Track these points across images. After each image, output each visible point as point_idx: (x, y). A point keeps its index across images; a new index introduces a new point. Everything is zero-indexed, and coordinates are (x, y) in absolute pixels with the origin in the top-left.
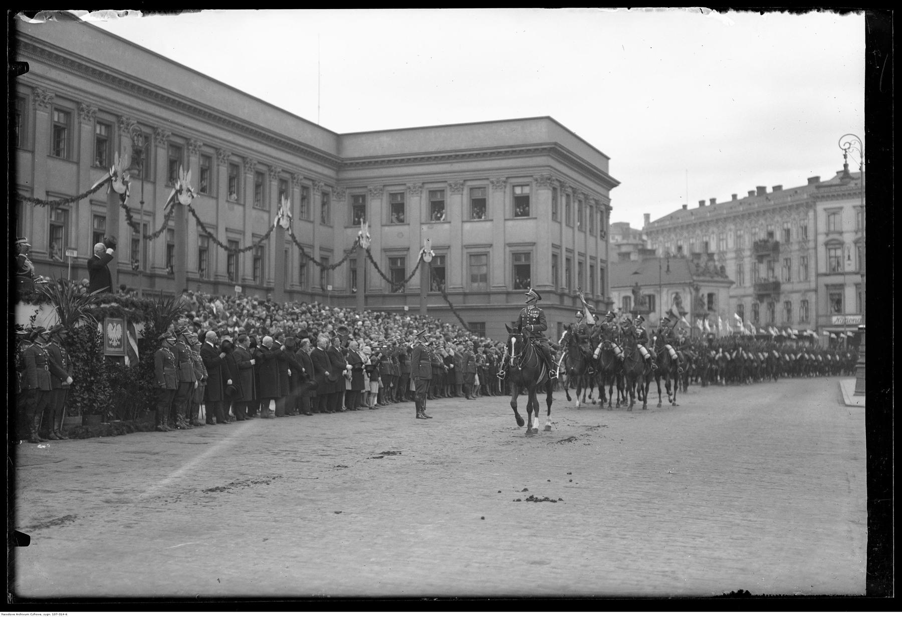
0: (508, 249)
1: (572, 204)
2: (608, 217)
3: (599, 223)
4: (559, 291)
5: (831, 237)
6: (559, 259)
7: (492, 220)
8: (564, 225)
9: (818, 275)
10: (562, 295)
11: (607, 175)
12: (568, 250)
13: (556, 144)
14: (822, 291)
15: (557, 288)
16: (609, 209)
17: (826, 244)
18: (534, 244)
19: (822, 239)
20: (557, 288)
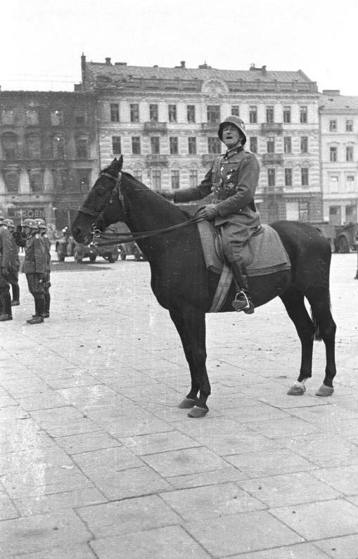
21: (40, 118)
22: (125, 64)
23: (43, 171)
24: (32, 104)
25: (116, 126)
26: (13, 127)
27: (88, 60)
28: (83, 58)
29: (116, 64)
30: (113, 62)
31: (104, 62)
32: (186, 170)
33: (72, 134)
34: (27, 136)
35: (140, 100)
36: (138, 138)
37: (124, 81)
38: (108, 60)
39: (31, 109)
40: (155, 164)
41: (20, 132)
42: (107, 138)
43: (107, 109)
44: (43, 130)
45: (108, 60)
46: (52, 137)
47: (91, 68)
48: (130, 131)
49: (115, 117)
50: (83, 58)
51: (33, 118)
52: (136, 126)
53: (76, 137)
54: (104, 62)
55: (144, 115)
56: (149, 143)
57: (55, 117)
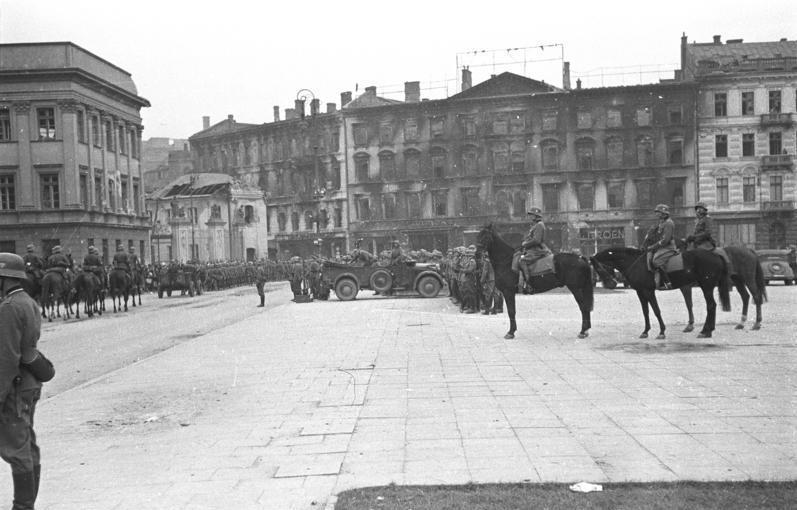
0: (34, 171)
1: (99, 125)
2: (140, 136)
3: (130, 145)
4: (89, 210)
5: (360, 150)
6: (88, 180)
7: (17, 142)
8: (91, 146)
9: (348, 186)
10: (93, 213)
11: (136, 96)
12: (97, 171)
13: (77, 69)
14: (351, 198)
15: (86, 206)
16: (140, 128)
17: (355, 157)
18: (60, 166)
19: (351, 152)
20: (86, 206)
21: (623, 119)
22: (741, 41)
23: (624, 182)
24: (615, 102)
25: (722, 121)
26: (590, 131)
27: (690, 41)
28: (684, 39)
29: (729, 42)
30: (723, 41)
31: (712, 41)
32: (737, 177)
33: (663, 136)
34: (606, 142)
35: (756, 87)
36: (751, 136)
37: (736, 63)
38: (717, 38)
39: (616, 108)
40: (776, 168)
41: (597, 137)
42: (709, 137)
43: (710, 100)
44: (628, 131)
45: (717, 38)
46: (638, 140)
47: (690, 51)
48: (740, 127)
49: (721, 110)
50: (684, 39)
51: (615, 118)
52: (748, 120)
53: (668, 138)
54: (712, 41)
55: (762, 104)
56: (767, 141)
57: (643, 117)
